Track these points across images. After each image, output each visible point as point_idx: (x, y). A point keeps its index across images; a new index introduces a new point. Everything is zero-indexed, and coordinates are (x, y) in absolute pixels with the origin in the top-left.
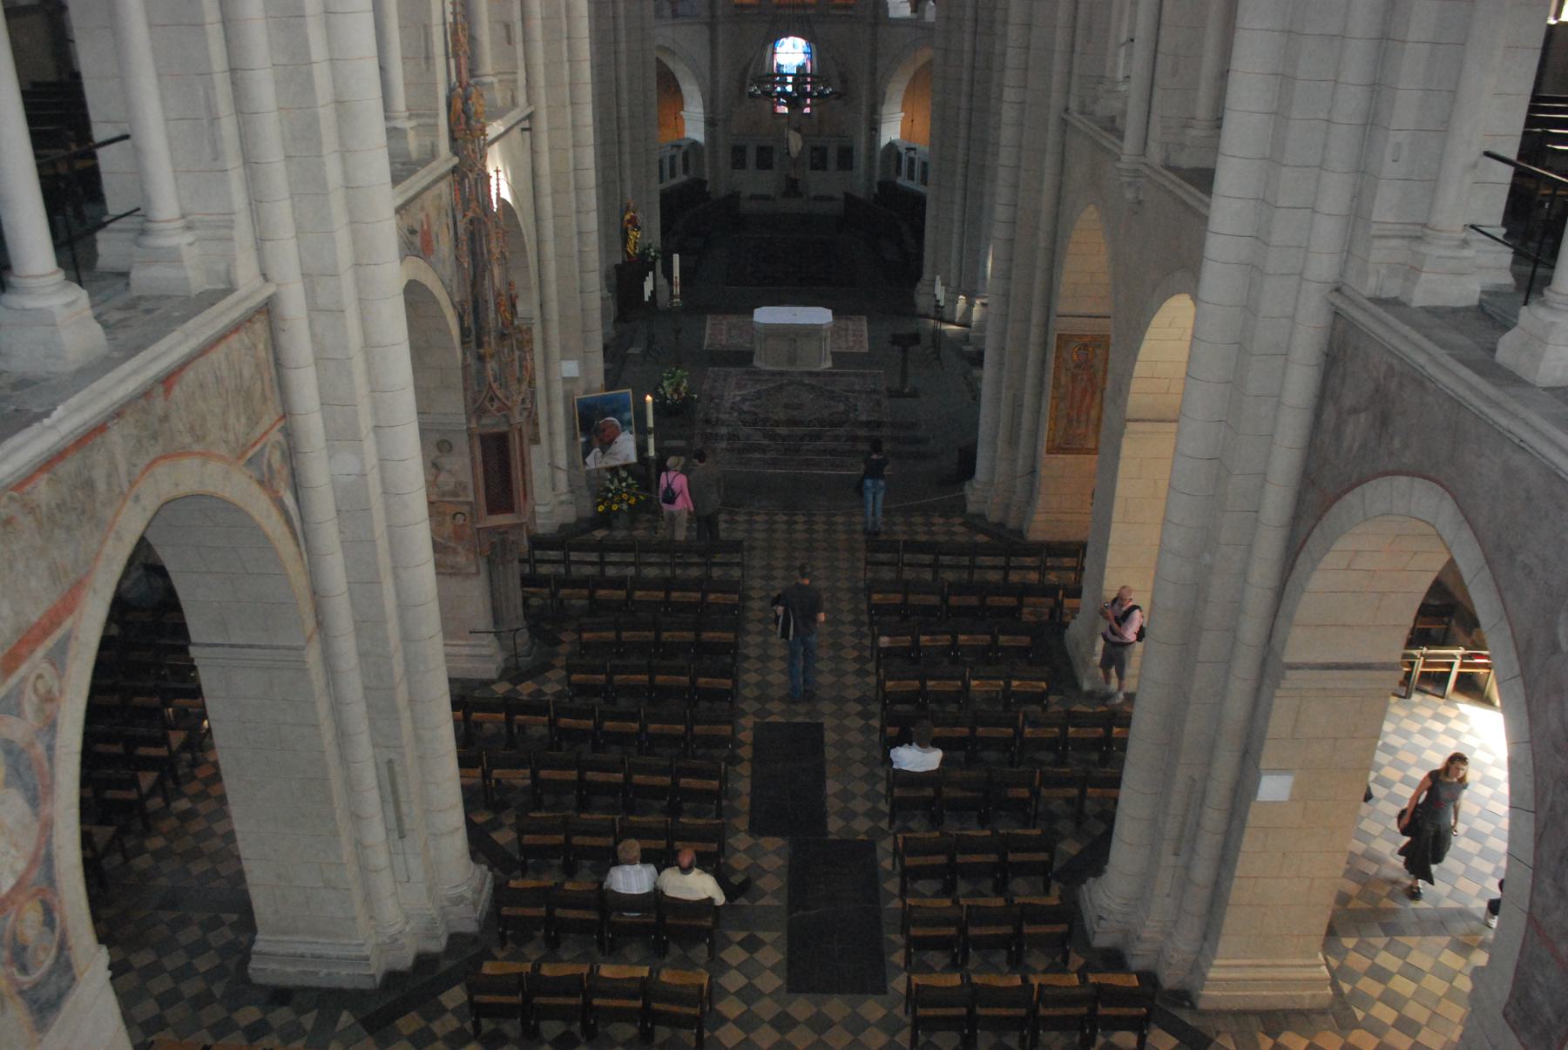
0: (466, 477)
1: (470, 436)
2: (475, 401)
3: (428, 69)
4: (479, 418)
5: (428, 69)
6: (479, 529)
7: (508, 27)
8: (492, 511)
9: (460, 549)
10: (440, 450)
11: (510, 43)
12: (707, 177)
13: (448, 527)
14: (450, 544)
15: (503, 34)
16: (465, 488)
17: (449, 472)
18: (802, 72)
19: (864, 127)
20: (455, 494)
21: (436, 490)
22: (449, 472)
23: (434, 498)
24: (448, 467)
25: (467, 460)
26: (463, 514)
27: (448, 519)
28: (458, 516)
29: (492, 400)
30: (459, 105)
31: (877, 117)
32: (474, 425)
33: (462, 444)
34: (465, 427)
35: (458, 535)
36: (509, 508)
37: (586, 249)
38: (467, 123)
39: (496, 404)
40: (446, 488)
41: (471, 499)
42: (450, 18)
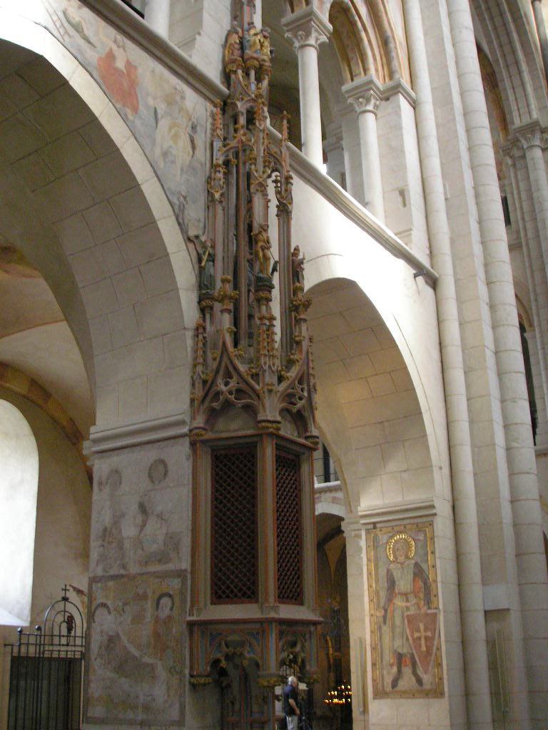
0: (181, 523)
1: (193, 444)
2: (205, 382)
6: (191, 625)
7: (402, 193)
8: (221, 594)
9: (161, 672)
11: (405, 205)
13: (146, 631)
14: (147, 660)
15: (400, 199)
16: (176, 547)
17: (160, 516)
20: (162, 558)
21: (140, 552)
22: (160, 516)
23: (134, 569)
24: (159, 508)
25: (185, 493)
26: (170, 596)
27: (149, 605)
28: (165, 601)
29: (228, 375)
30: (235, 39)
32: (200, 421)
33: (179, 456)
35: (159, 643)
36: (249, 593)
37: (515, 444)
39: (233, 383)
40: (154, 548)
41: (185, 564)
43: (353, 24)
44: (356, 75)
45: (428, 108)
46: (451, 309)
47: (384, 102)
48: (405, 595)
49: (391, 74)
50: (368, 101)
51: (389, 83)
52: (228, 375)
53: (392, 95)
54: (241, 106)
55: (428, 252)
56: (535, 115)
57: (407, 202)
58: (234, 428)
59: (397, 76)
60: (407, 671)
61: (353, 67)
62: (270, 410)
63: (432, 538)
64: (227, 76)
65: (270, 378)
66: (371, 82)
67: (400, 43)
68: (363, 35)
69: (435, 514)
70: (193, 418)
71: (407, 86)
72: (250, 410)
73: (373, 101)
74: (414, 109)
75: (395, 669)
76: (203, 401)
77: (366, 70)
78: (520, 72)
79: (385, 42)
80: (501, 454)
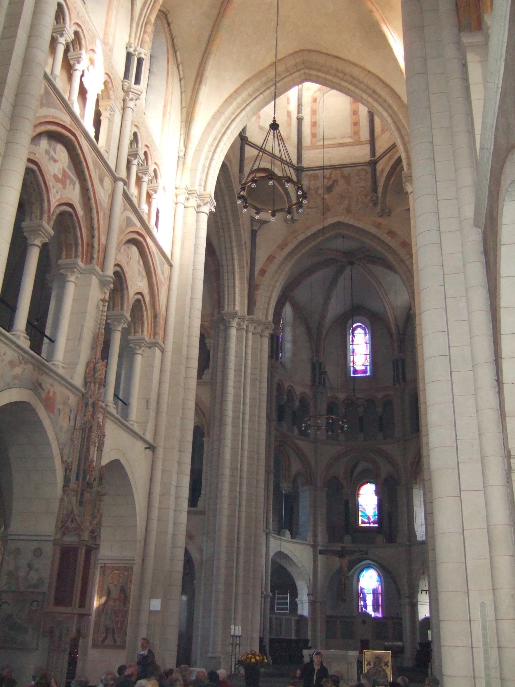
1: (54, 544)
3: (78, 345)
4: (64, 534)
5: (78, 345)
7: (147, 401)
10: (35, 555)
11: (147, 409)
12: (309, 638)
18: (376, 592)
19: (408, 608)
29: (72, 521)
30: (92, 366)
31: (414, 601)
32: (59, 536)
34: (52, 539)
38: (94, 375)
39: (74, 525)
42: (97, 331)
43: (142, 307)
44: (136, 332)
45: (169, 355)
46: (159, 464)
47: (147, 349)
48: (115, 600)
49: (155, 334)
50: (141, 347)
51: (152, 340)
52: (72, 521)
53: (152, 346)
54: (91, 401)
55: (154, 432)
56: (237, 308)
57: (149, 407)
58: (70, 539)
59: (157, 337)
60: (110, 636)
61: (136, 327)
62: (86, 536)
63: (132, 575)
64: (86, 383)
65: (88, 524)
66: (144, 339)
67: (163, 316)
68: (145, 313)
69: (135, 564)
70: (56, 534)
71: (160, 342)
72: (79, 535)
73: (143, 348)
74: (162, 352)
75: (104, 635)
76: (61, 528)
77: (143, 331)
78: (234, 279)
79: (155, 316)
80: (169, 537)
